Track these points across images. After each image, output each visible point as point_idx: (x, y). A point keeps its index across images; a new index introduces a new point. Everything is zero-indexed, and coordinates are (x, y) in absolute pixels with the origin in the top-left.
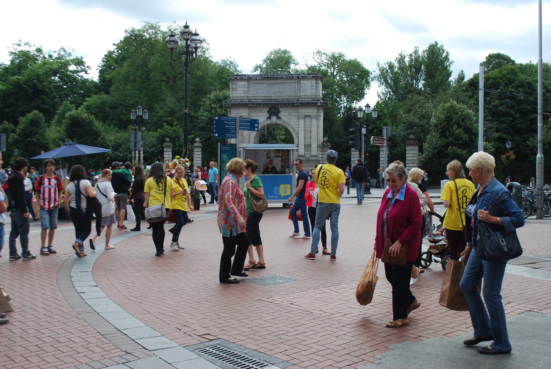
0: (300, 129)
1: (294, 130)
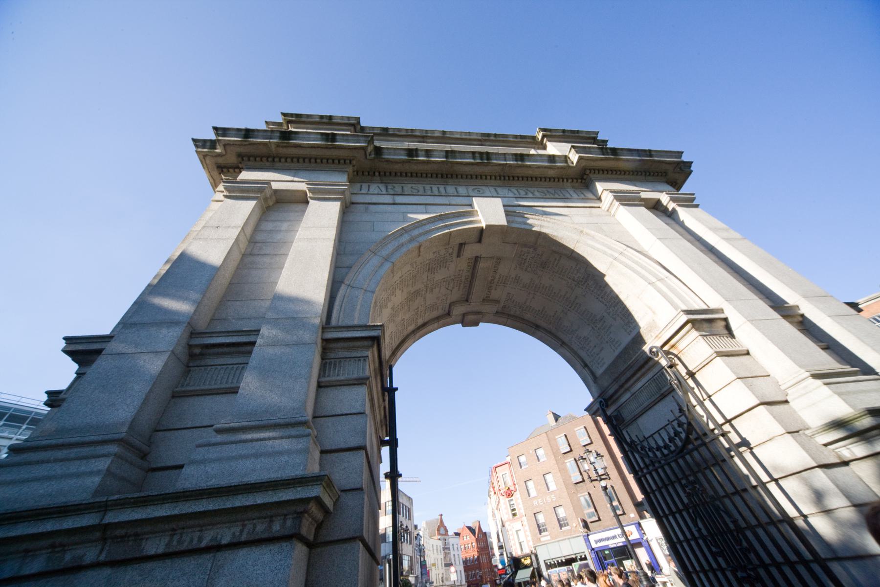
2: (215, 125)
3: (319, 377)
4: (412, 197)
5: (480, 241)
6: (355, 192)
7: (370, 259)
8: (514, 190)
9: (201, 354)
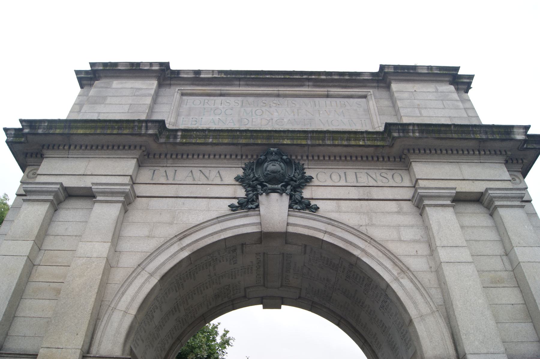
0: (443, 255)
1: (405, 270)
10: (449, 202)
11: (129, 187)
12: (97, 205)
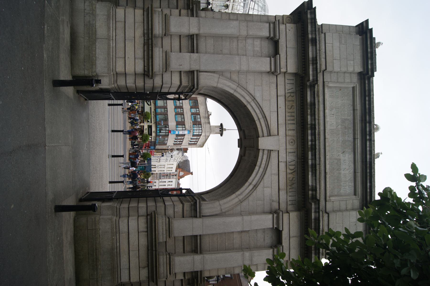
2: (316, 8)
3: (183, 71)
4: (284, 105)
5: (257, 137)
6: (286, 77)
7: (234, 85)
8: (293, 163)
9: (192, 38)
10: (275, 226)
11: (279, 72)
12: (269, 59)
